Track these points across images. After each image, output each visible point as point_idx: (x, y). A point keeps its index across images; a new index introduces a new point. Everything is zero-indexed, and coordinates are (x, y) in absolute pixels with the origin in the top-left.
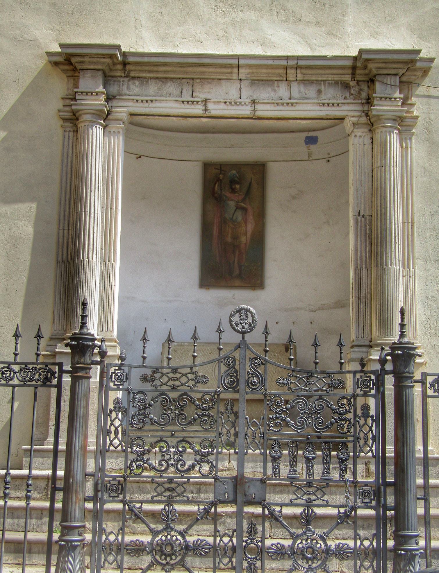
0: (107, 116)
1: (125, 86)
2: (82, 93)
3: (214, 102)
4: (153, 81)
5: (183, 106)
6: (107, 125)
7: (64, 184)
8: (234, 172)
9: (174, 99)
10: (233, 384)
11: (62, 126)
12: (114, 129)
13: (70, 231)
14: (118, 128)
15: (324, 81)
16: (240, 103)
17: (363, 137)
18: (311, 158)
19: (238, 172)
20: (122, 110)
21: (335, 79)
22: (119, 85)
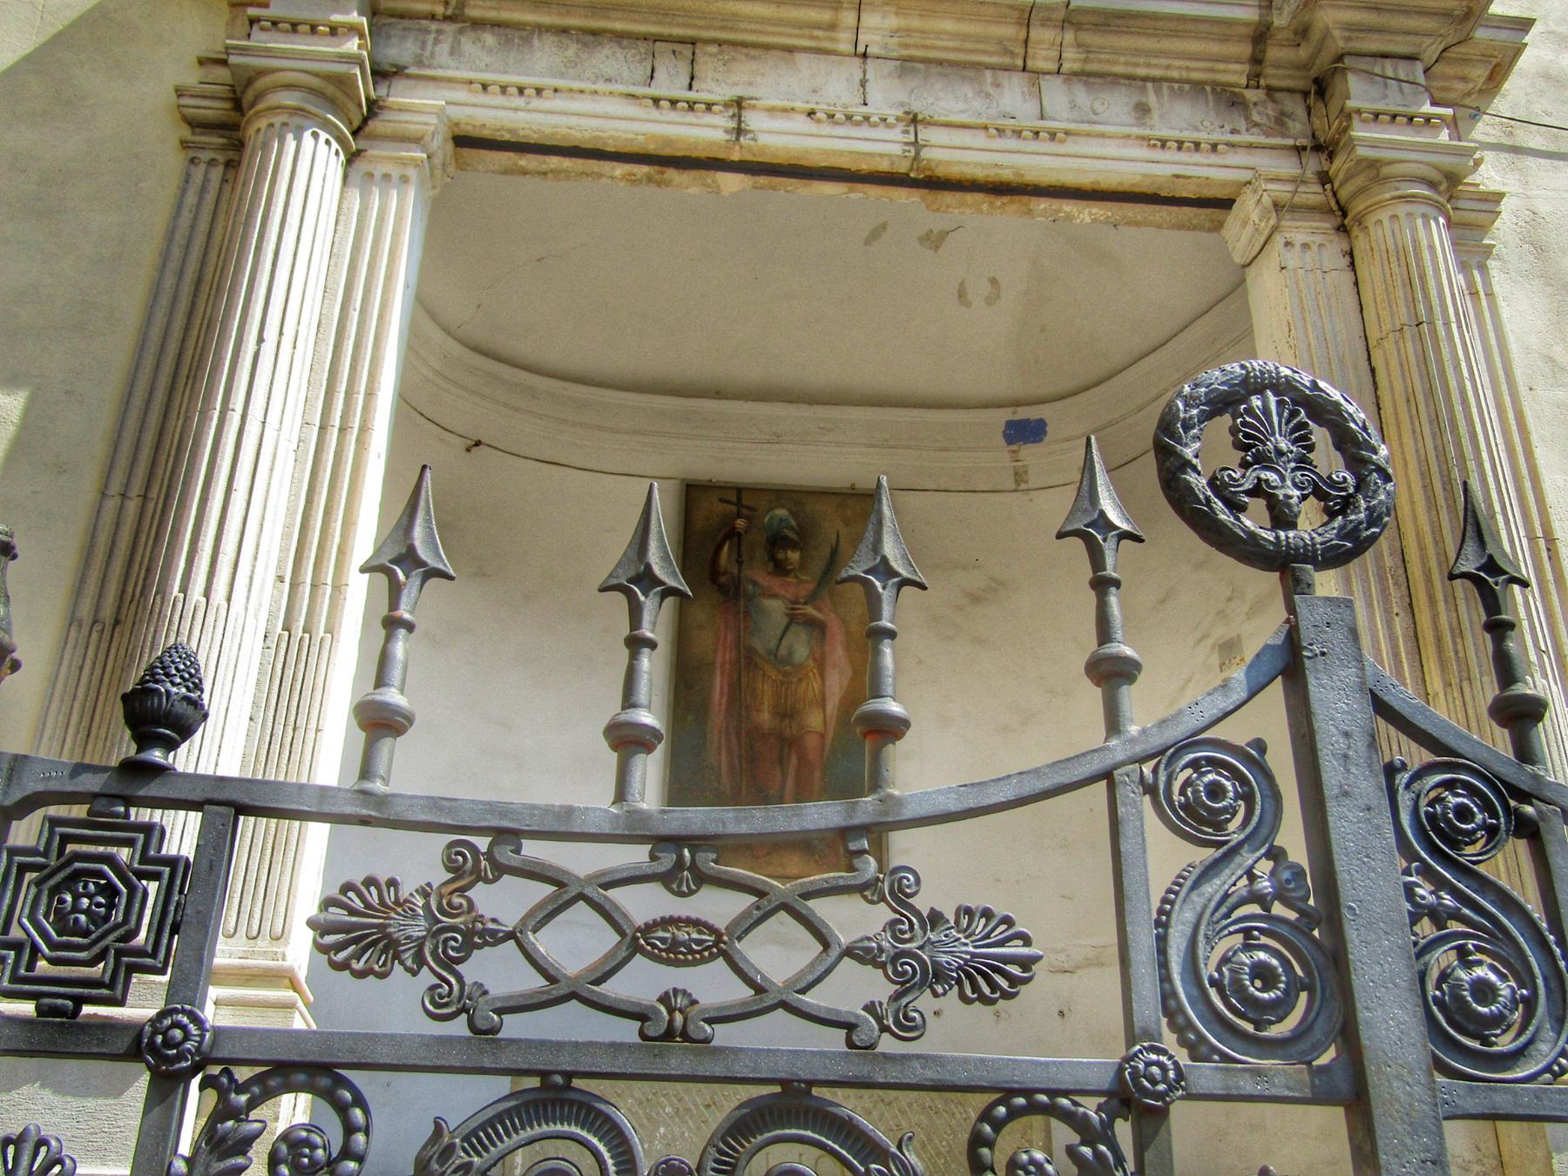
0: (365, 120)
1: (444, 48)
2: (275, 24)
3: (771, 110)
4: (549, 39)
5: (654, 114)
6: (359, 152)
7: (155, 333)
8: (782, 512)
9: (622, 88)
10: (1281, 1008)
11: (185, 145)
12: (387, 168)
13: (151, 506)
14: (403, 163)
15: (1154, 80)
16: (867, 118)
17: (1314, 248)
18: (1023, 486)
19: (794, 514)
20: (423, 106)
21: (1195, 76)
22: (424, 44)
